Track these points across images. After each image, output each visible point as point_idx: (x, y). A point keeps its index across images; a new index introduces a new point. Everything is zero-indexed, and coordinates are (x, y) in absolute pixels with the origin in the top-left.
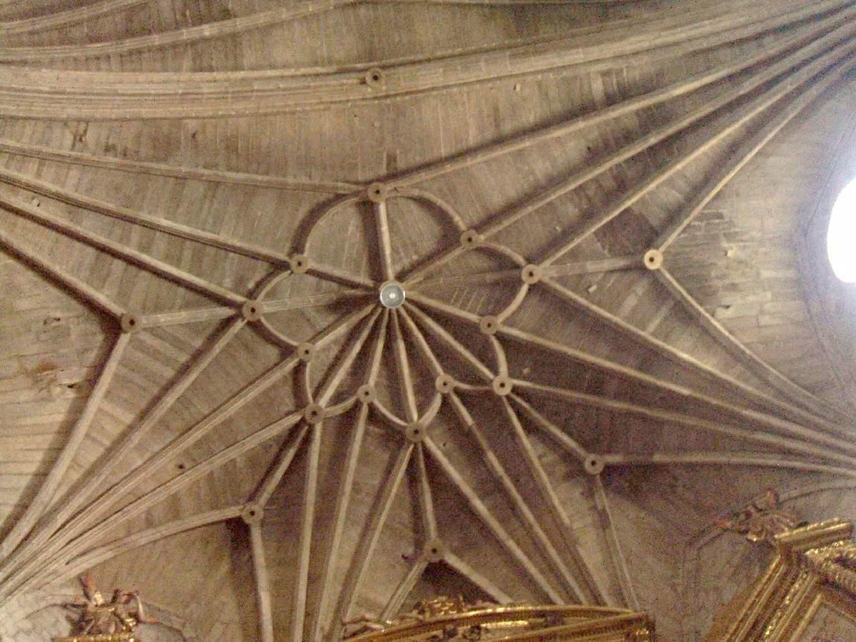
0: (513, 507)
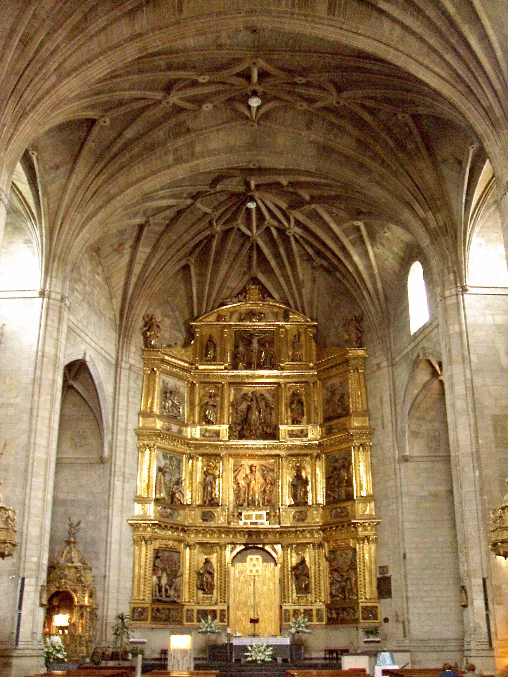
0: (285, 267)
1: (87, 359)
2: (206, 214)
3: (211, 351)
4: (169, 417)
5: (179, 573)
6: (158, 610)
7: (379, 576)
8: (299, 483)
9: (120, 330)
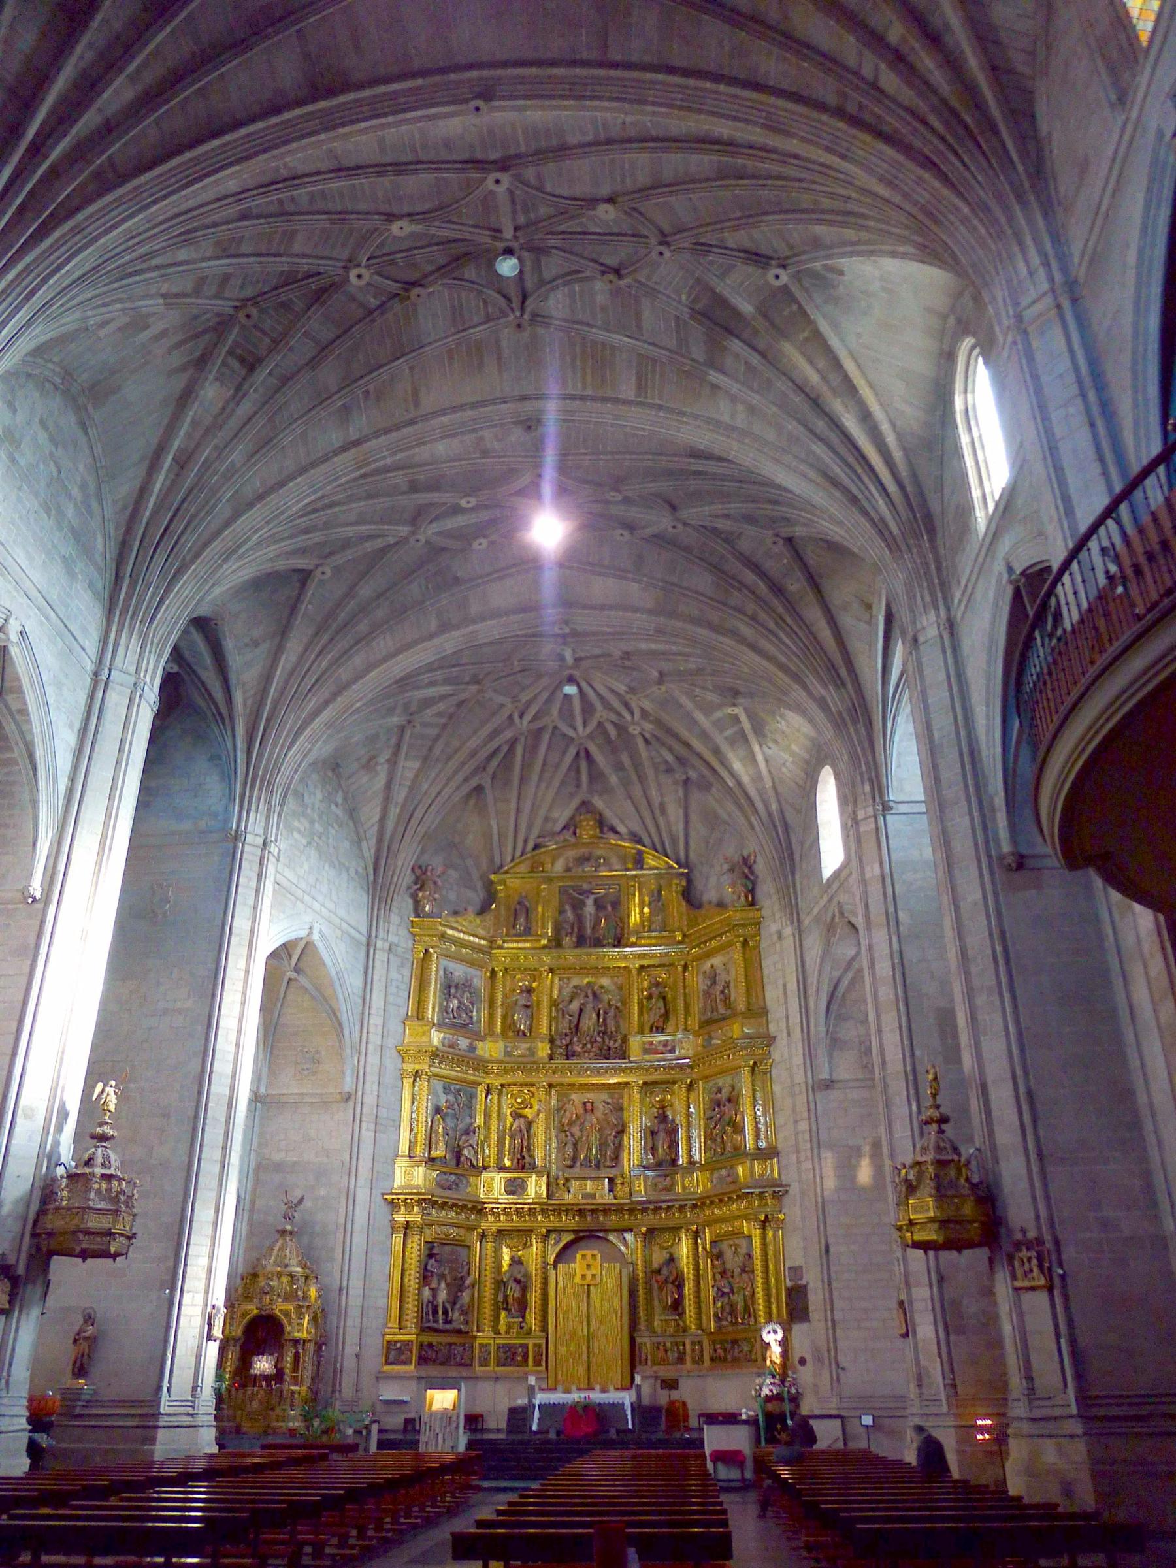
1: (316, 937)
2: (502, 705)
3: (522, 920)
4: (454, 1026)
5: (468, 1282)
6: (430, 1345)
7: (789, 1284)
8: (663, 1129)
9: (374, 889)
